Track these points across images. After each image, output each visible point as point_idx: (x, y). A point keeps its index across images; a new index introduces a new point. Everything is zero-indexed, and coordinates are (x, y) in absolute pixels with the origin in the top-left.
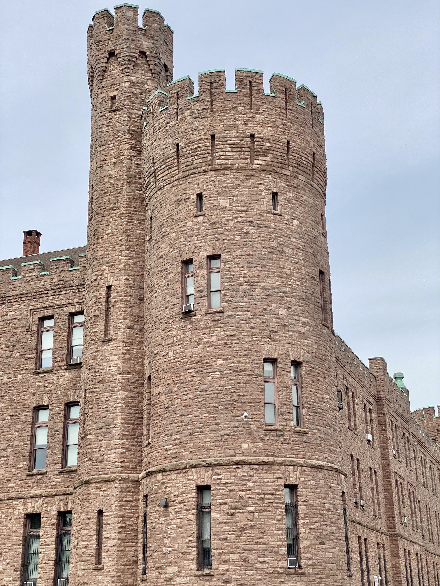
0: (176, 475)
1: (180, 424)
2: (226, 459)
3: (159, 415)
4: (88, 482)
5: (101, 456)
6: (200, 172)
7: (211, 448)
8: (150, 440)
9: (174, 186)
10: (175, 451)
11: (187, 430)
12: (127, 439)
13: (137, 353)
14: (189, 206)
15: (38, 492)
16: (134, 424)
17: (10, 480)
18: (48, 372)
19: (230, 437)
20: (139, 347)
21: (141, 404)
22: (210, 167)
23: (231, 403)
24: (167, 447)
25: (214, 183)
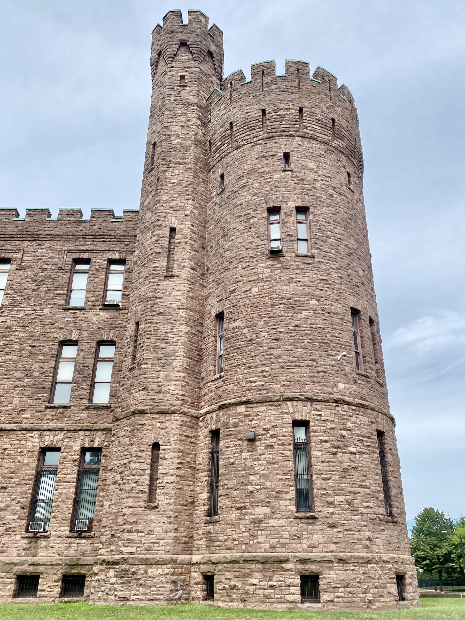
0: (265, 408)
1: (269, 357)
2: (327, 397)
3: (238, 349)
4: (143, 412)
5: (159, 386)
6: (287, 136)
7: (308, 383)
8: (222, 374)
9: (257, 145)
10: (262, 383)
11: (278, 362)
12: (188, 373)
13: (198, 294)
14: (275, 162)
15: (60, 425)
16: (193, 360)
17: (25, 411)
18: (80, 309)
19: (327, 374)
20: (200, 289)
21: (200, 342)
22: (298, 133)
23: (326, 341)
24: (251, 379)
25: (301, 147)
